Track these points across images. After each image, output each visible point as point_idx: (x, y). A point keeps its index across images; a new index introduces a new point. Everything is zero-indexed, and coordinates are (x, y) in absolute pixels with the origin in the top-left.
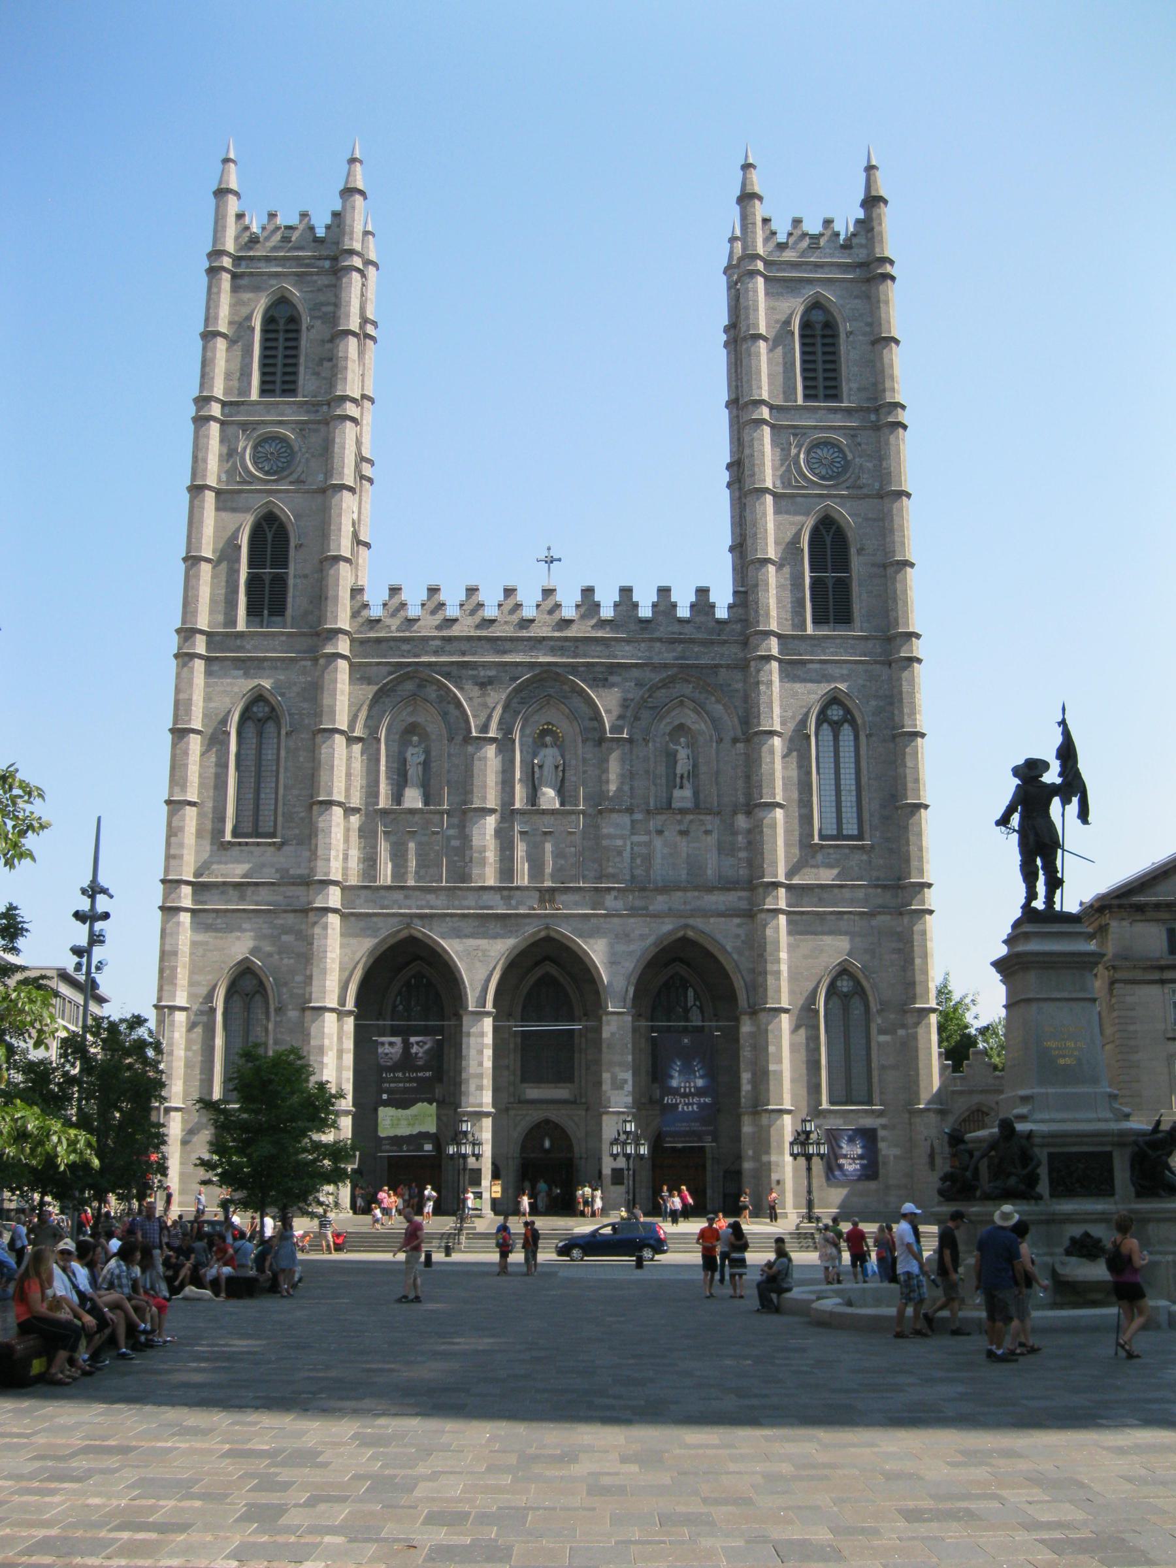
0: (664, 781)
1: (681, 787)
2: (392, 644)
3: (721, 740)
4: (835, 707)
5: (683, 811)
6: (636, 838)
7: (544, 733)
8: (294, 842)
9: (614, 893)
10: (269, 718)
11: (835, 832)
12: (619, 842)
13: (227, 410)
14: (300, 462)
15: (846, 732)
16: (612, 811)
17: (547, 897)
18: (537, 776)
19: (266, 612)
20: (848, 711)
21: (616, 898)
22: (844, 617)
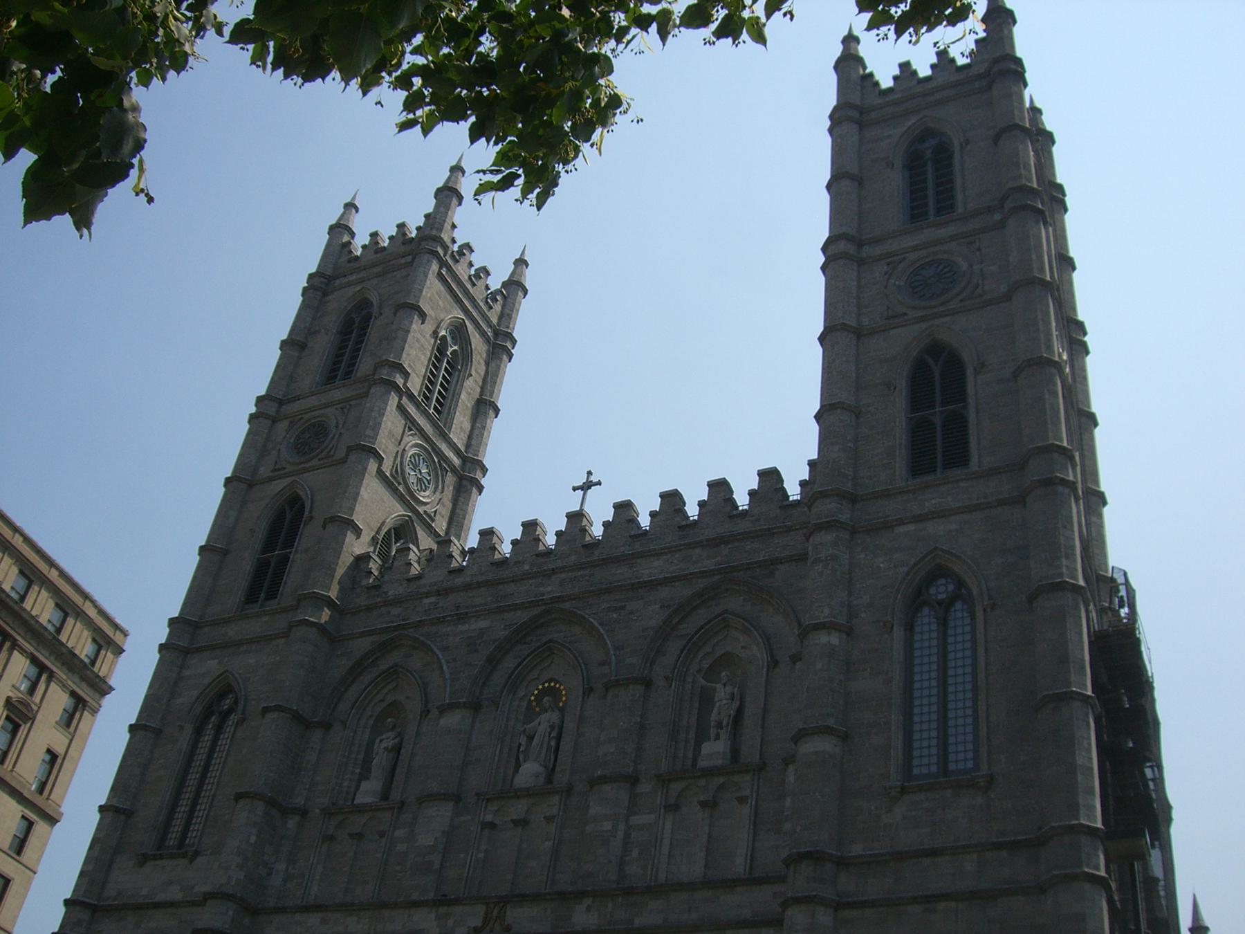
0: (692, 735)
1: (717, 737)
2: (384, 610)
3: (776, 663)
4: (942, 581)
5: (709, 773)
6: (636, 820)
7: (544, 692)
8: (209, 852)
9: (588, 901)
10: (231, 710)
11: (934, 769)
12: (607, 826)
13: (283, 408)
14: (333, 438)
15: (959, 614)
16: (603, 780)
17: (495, 913)
18: (522, 749)
19: (262, 595)
20: (960, 584)
21: (589, 909)
22: (957, 455)
